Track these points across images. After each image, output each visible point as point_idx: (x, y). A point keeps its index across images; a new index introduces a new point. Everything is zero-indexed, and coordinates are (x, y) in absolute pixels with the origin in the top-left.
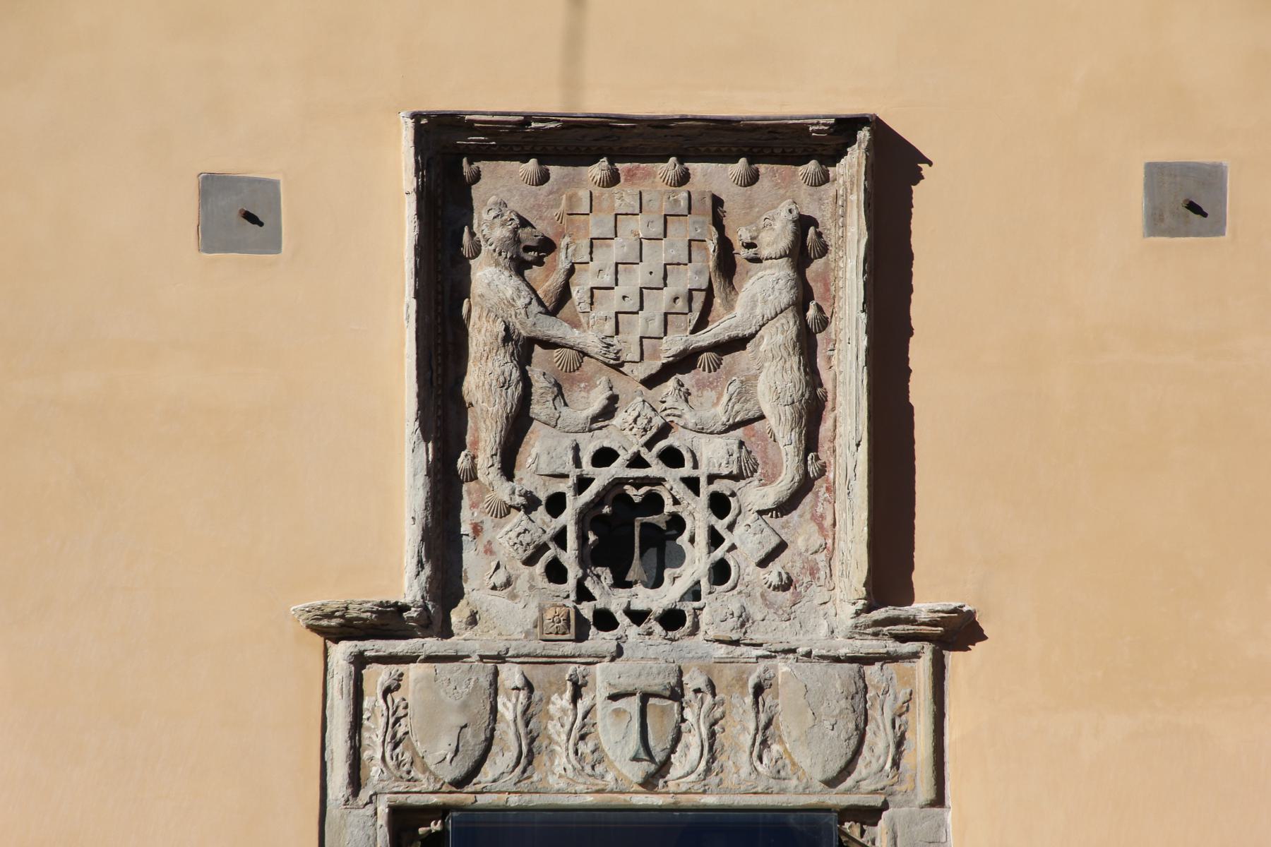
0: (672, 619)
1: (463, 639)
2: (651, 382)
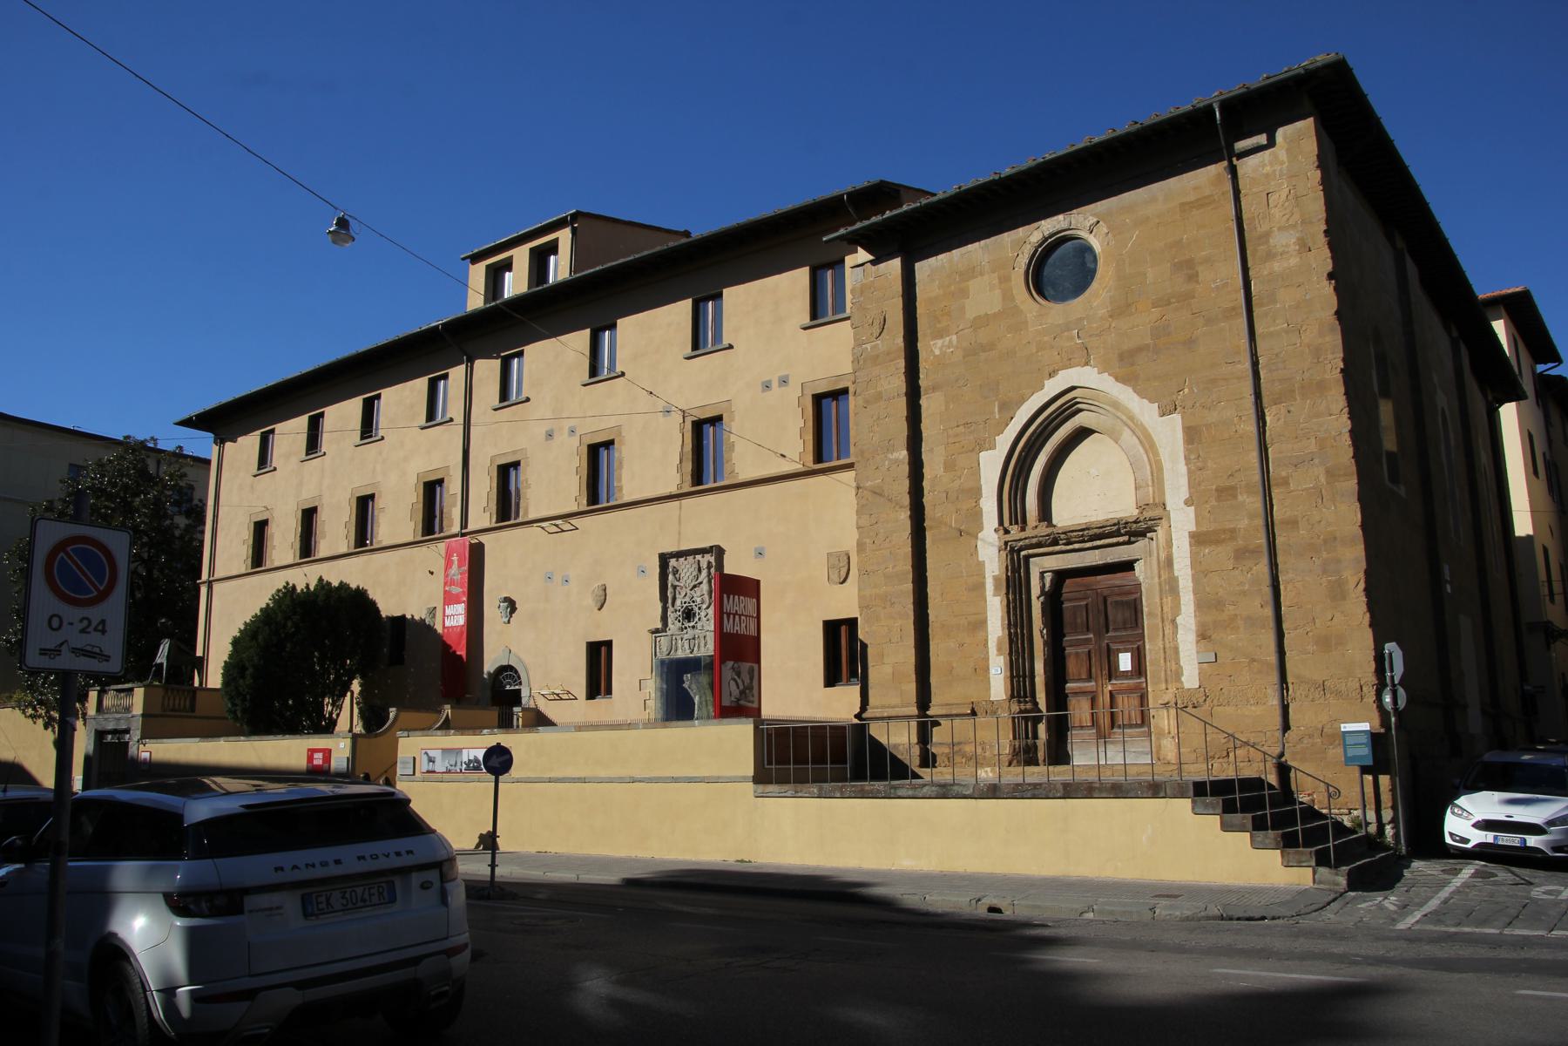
0: (693, 627)
1: (669, 633)
2: (691, 590)
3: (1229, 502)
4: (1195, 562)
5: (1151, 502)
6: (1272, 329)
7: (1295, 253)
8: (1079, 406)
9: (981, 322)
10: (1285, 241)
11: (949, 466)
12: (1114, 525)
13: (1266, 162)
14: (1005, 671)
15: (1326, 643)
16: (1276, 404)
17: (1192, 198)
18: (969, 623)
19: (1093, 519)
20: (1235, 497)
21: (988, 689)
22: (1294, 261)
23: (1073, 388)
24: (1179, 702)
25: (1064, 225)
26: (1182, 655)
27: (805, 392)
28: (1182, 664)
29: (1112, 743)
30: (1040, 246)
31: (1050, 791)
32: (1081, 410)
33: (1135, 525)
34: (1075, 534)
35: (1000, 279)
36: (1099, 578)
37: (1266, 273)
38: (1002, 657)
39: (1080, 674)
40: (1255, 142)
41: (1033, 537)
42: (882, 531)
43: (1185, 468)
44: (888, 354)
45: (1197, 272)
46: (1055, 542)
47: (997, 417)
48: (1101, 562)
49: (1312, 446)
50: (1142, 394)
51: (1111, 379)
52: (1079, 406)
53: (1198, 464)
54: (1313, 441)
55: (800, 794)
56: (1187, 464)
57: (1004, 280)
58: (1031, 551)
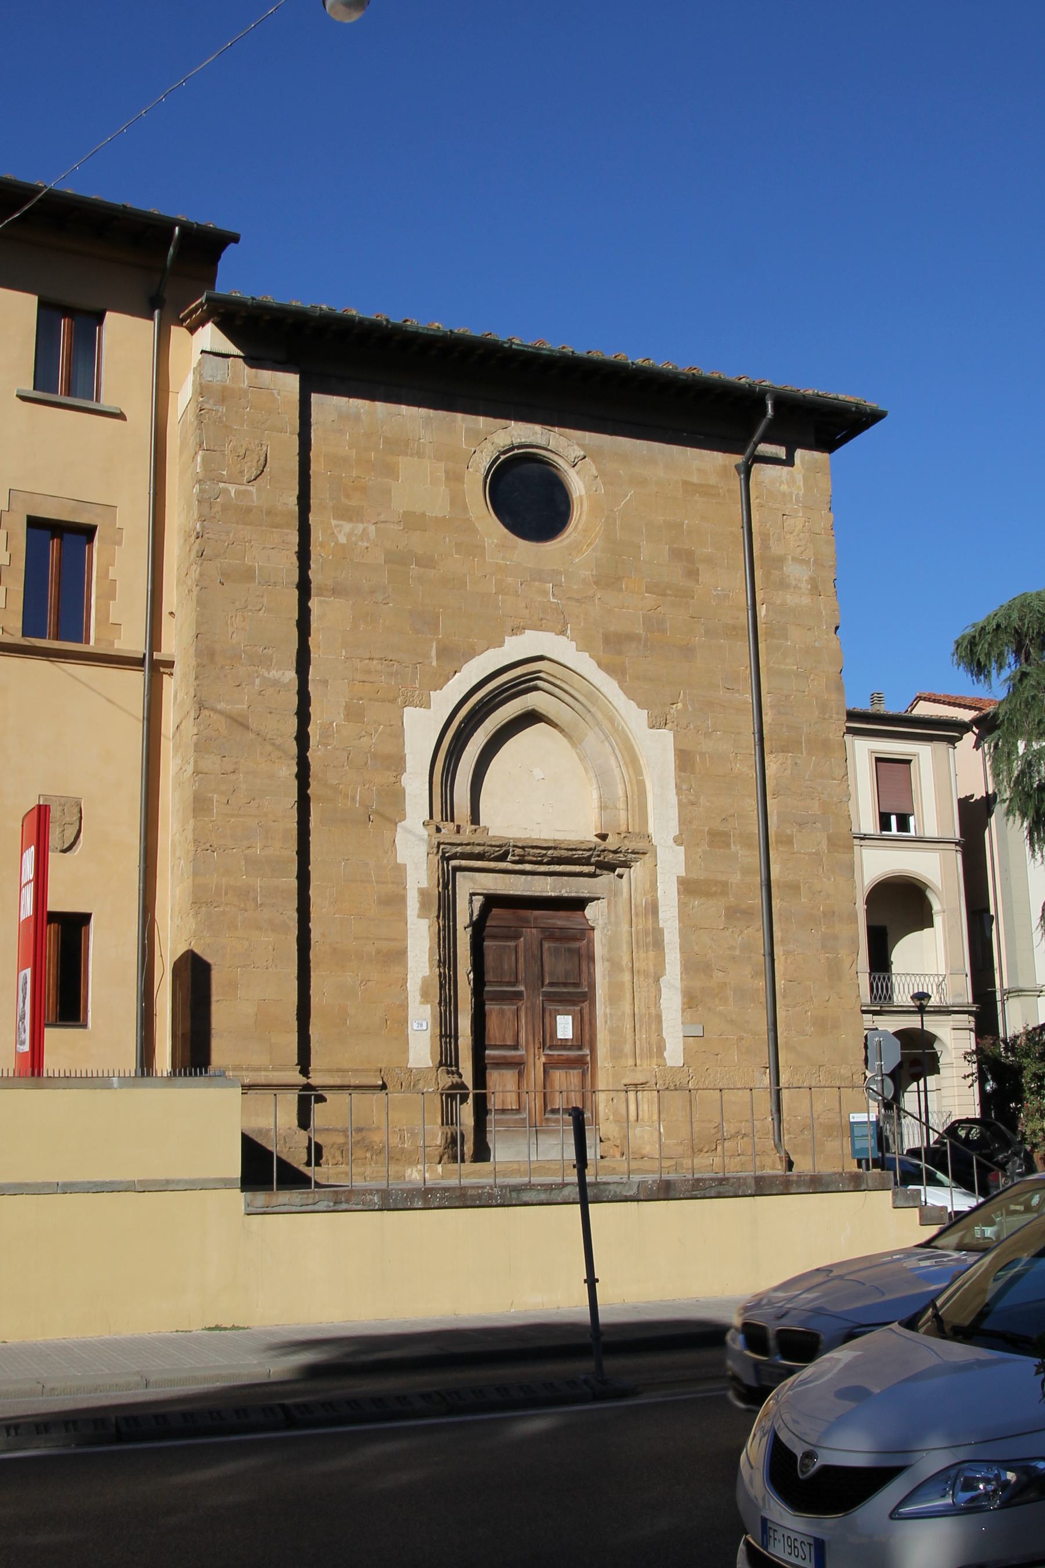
3: (722, 850)
4: (684, 915)
5: (623, 828)
6: (783, 667)
7: (807, 592)
8: (540, 683)
9: (413, 522)
10: (797, 573)
11: (354, 713)
12: (590, 850)
13: (784, 478)
14: (433, 1029)
15: (824, 1025)
16: (783, 752)
17: (695, 479)
18: (378, 952)
19: (535, 835)
20: (728, 845)
21: (405, 1050)
22: (806, 600)
23: (541, 658)
24: (660, 1082)
25: (540, 440)
26: (664, 1025)
27: (13, 506)
28: (664, 1036)
29: (545, 1132)
30: (504, 453)
31: (739, 1187)
32: (536, 688)
33: (611, 856)
34: (539, 851)
35: (447, 472)
36: (537, 913)
37: (778, 602)
38: (429, 1006)
39: (504, 1039)
40: (774, 451)
41: (479, 845)
42: (243, 787)
43: (676, 798)
44: (269, 513)
45: (698, 570)
46: (502, 858)
47: (434, 663)
48: (553, 894)
49: (815, 808)
50: (630, 693)
51: (593, 664)
52: (540, 683)
53: (692, 797)
54: (817, 803)
55: (344, 1206)
56: (678, 794)
57: (455, 478)
58: (464, 863)
